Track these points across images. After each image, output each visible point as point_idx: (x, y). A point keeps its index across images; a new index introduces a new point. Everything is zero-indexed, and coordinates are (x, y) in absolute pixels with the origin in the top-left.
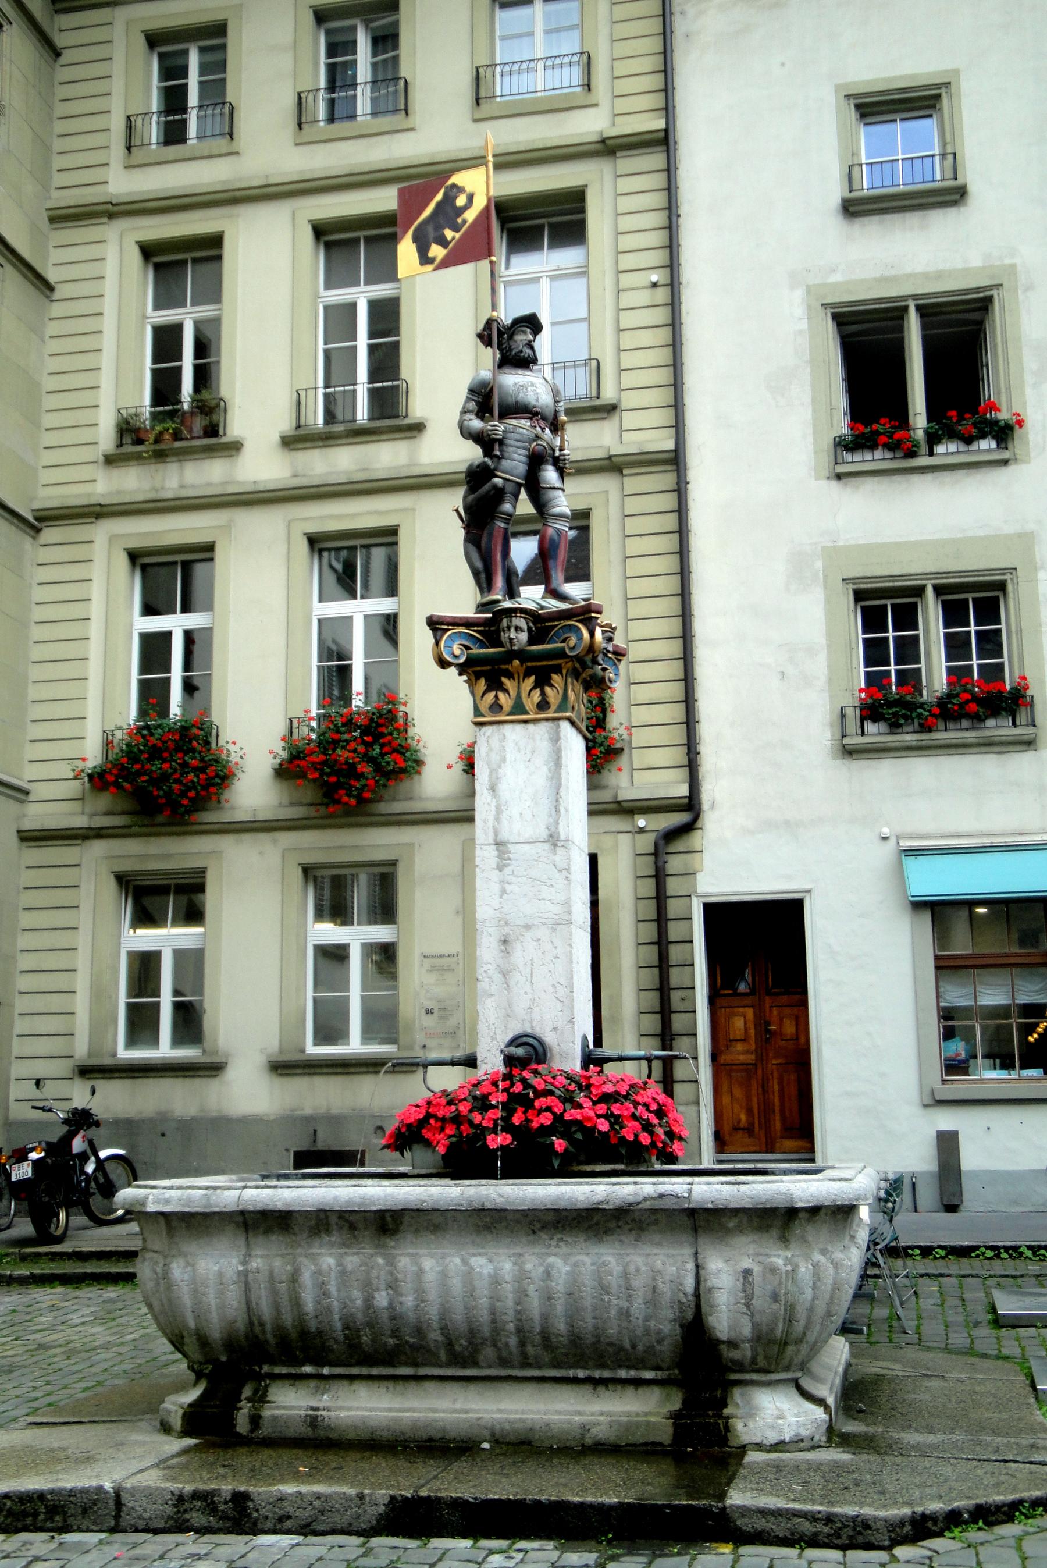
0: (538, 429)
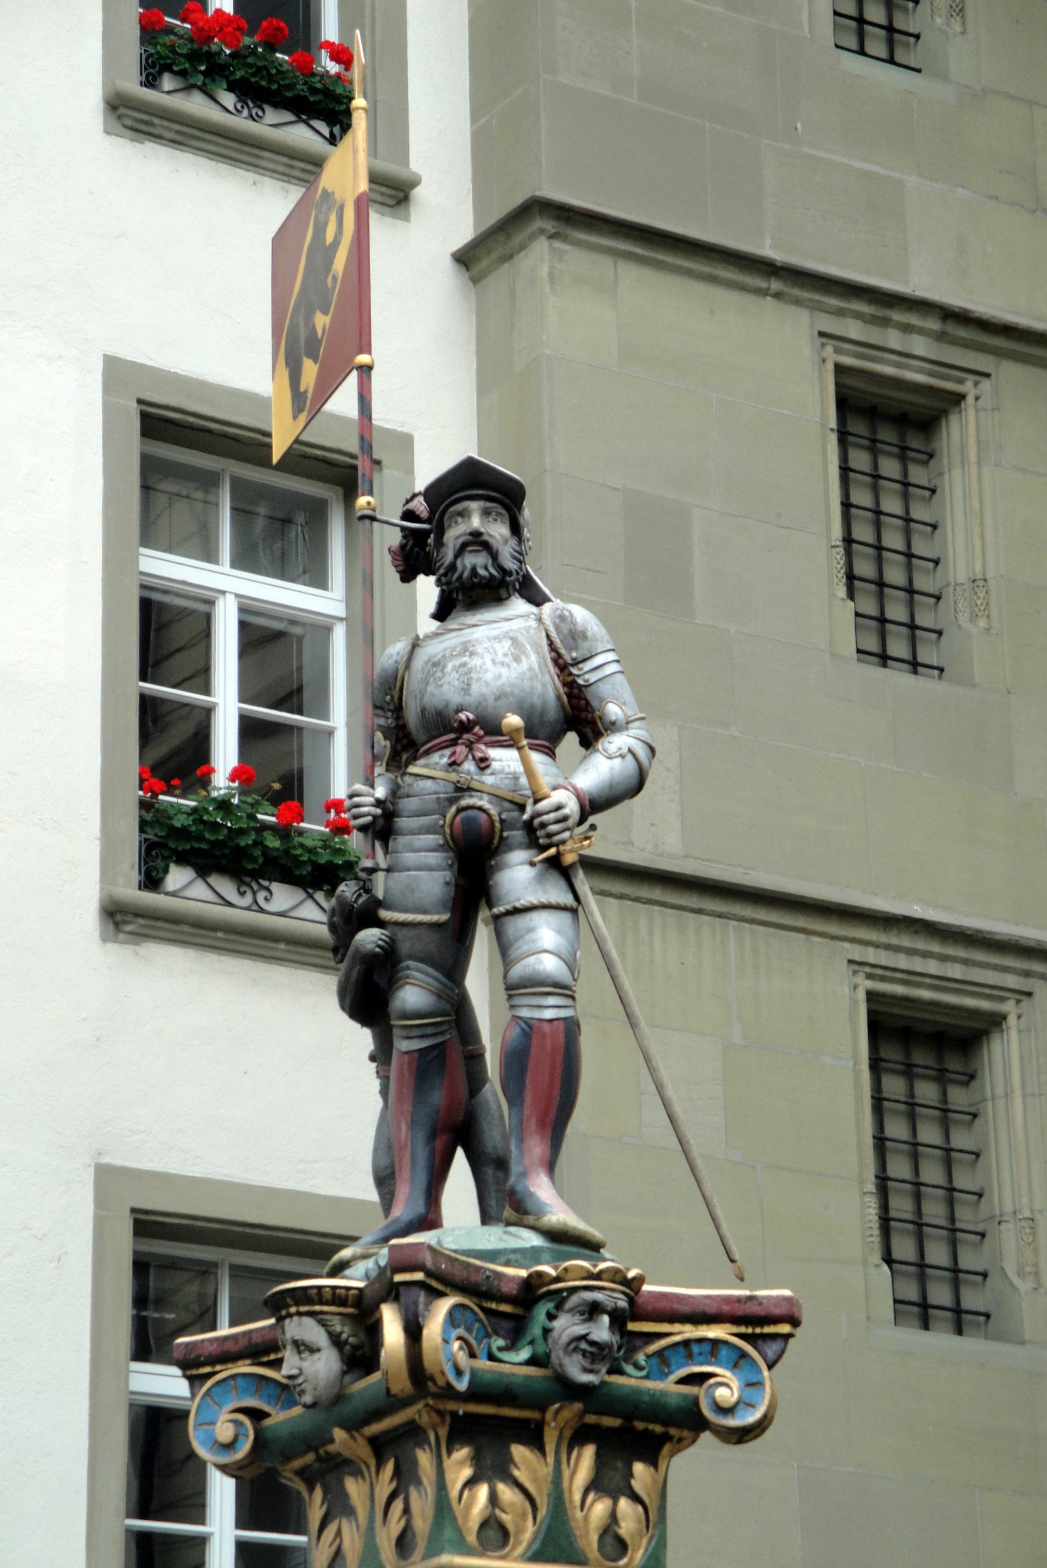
0: (469, 766)
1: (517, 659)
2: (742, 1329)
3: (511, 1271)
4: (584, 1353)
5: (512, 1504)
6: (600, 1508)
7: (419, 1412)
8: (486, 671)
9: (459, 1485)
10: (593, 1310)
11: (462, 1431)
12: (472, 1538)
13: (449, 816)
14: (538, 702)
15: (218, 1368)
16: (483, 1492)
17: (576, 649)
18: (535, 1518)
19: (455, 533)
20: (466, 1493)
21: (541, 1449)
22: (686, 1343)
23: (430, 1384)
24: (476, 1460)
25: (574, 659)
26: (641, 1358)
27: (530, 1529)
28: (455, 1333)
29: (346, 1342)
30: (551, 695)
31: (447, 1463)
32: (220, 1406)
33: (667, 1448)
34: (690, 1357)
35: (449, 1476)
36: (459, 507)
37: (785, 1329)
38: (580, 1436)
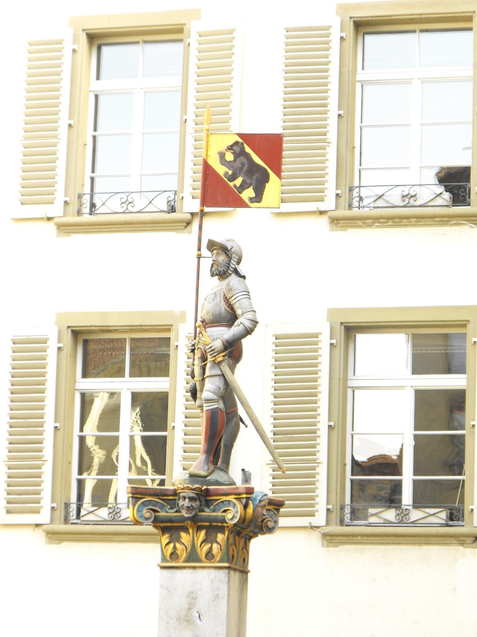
2: (237, 497)
6: (206, 547)
12: (168, 558)
14: (217, 313)
22: (223, 502)
24: (170, 537)
26: (212, 507)
27: (185, 555)
28: (145, 508)
30: (223, 309)
34: (224, 506)
38: (199, 528)
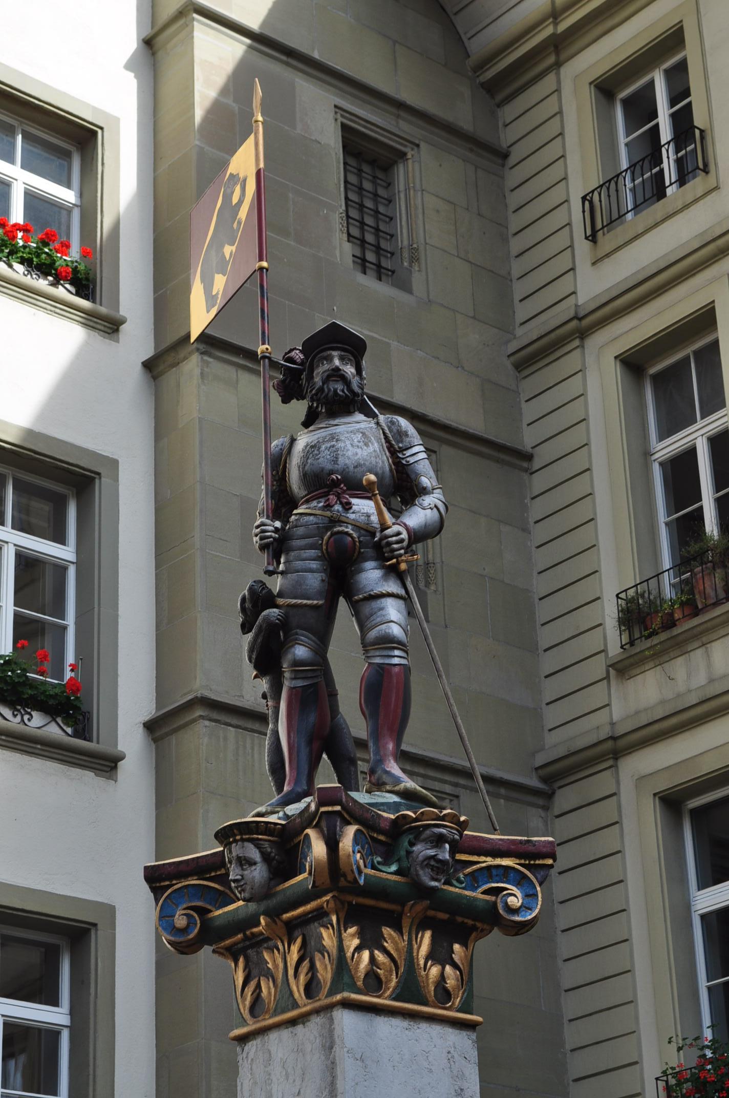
0: (338, 507)
1: (366, 445)
2: (523, 861)
3: (385, 815)
4: (433, 868)
5: (384, 963)
6: (435, 971)
7: (328, 901)
8: (348, 450)
9: (352, 950)
10: (439, 841)
11: (351, 916)
12: (360, 983)
13: (326, 538)
15: (174, 882)
16: (366, 955)
17: (402, 442)
18: (397, 974)
19: (322, 370)
20: (356, 955)
21: (399, 930)
22: (489, 868)
23: (342, 879)
24: (361, 934)
25: (400, 448)
27: (394, 980)
28: (357, 848)
29: (274, 858)
30: (387, 469)
31: (344, 935)
32: (177, 906)
33: (474, 935)
34: (491, 879)
35: (346, 943)
36: (325, 354)
37: (550, 862)
38: (423, 925)
